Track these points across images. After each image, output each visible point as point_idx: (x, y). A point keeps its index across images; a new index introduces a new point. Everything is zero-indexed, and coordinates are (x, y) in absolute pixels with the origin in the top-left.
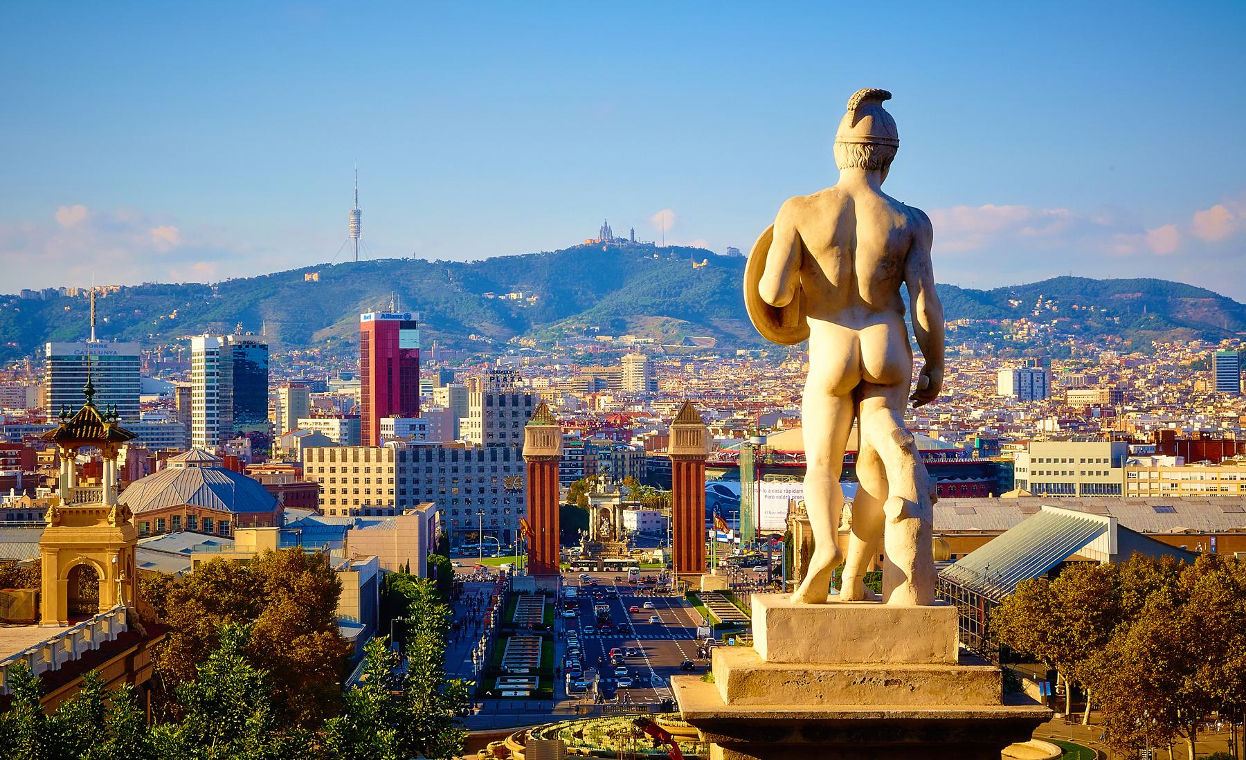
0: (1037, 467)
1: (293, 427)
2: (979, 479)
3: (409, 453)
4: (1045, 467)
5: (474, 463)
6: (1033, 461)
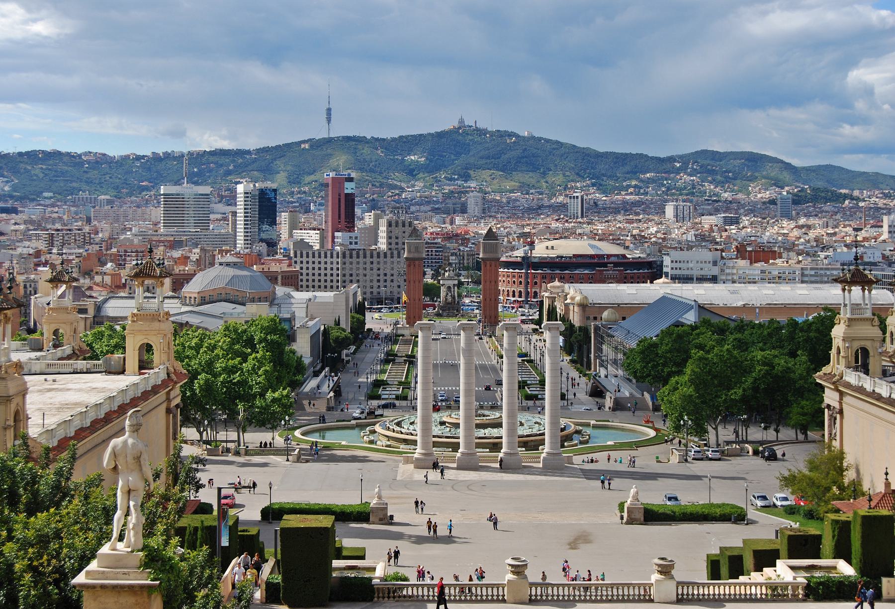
0: (675, 265)
1: (291, 235)
2: (646, 271)
3: (348, 253)
4: (678, 265)
5: (382, 259)
6: (672, 262)
